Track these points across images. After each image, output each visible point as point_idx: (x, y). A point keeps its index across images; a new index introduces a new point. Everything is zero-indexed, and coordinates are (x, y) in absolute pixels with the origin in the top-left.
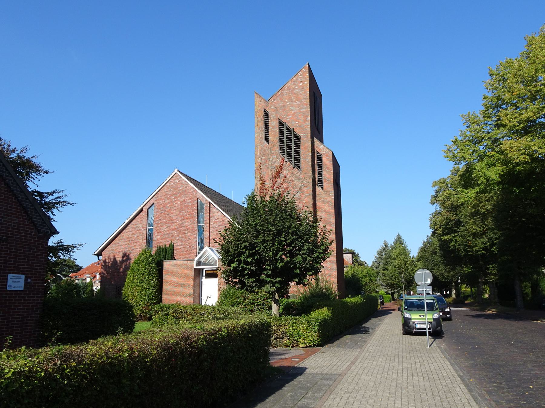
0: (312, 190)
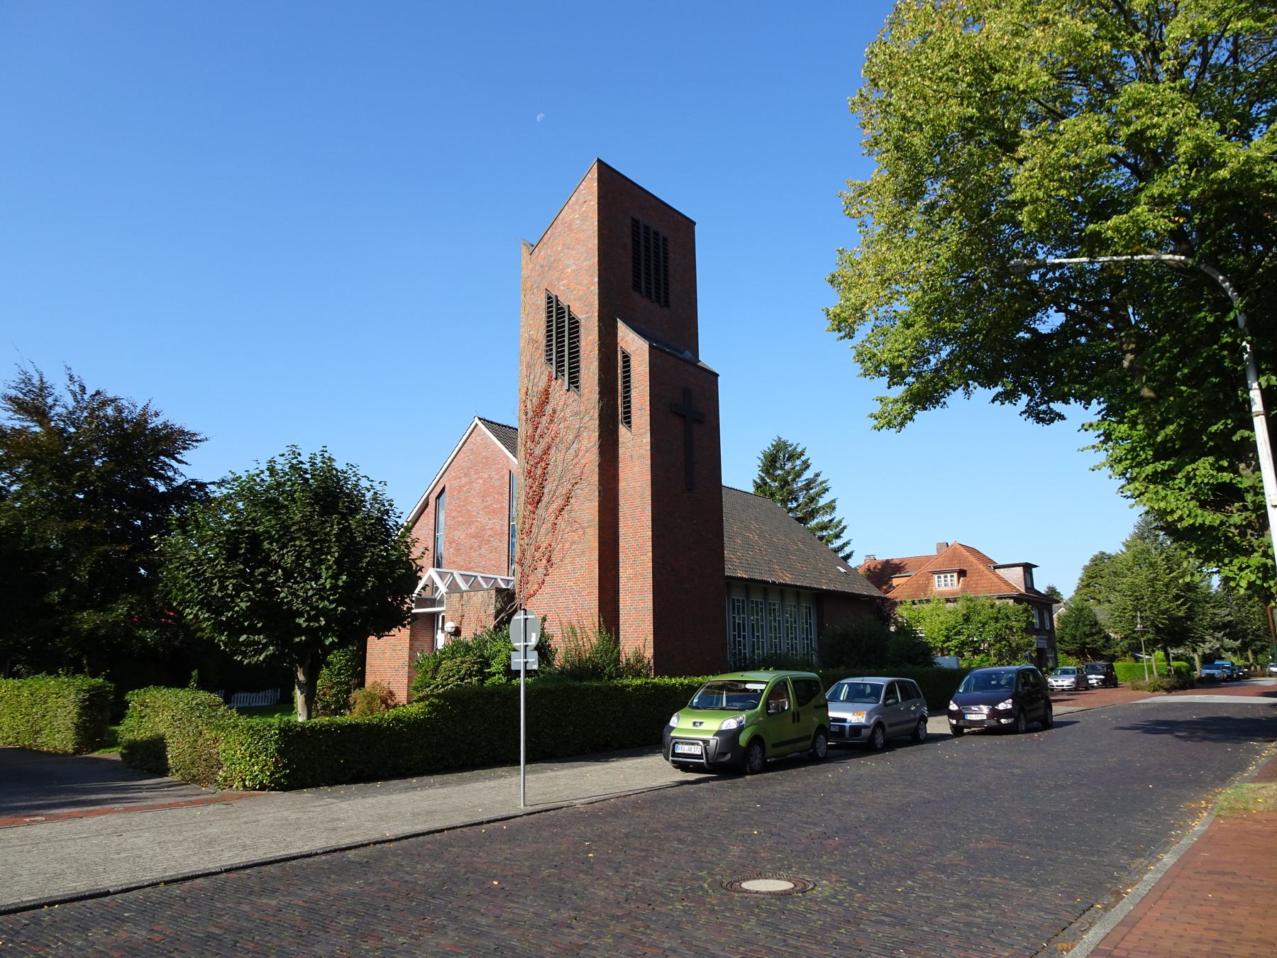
0: (597, 434)
